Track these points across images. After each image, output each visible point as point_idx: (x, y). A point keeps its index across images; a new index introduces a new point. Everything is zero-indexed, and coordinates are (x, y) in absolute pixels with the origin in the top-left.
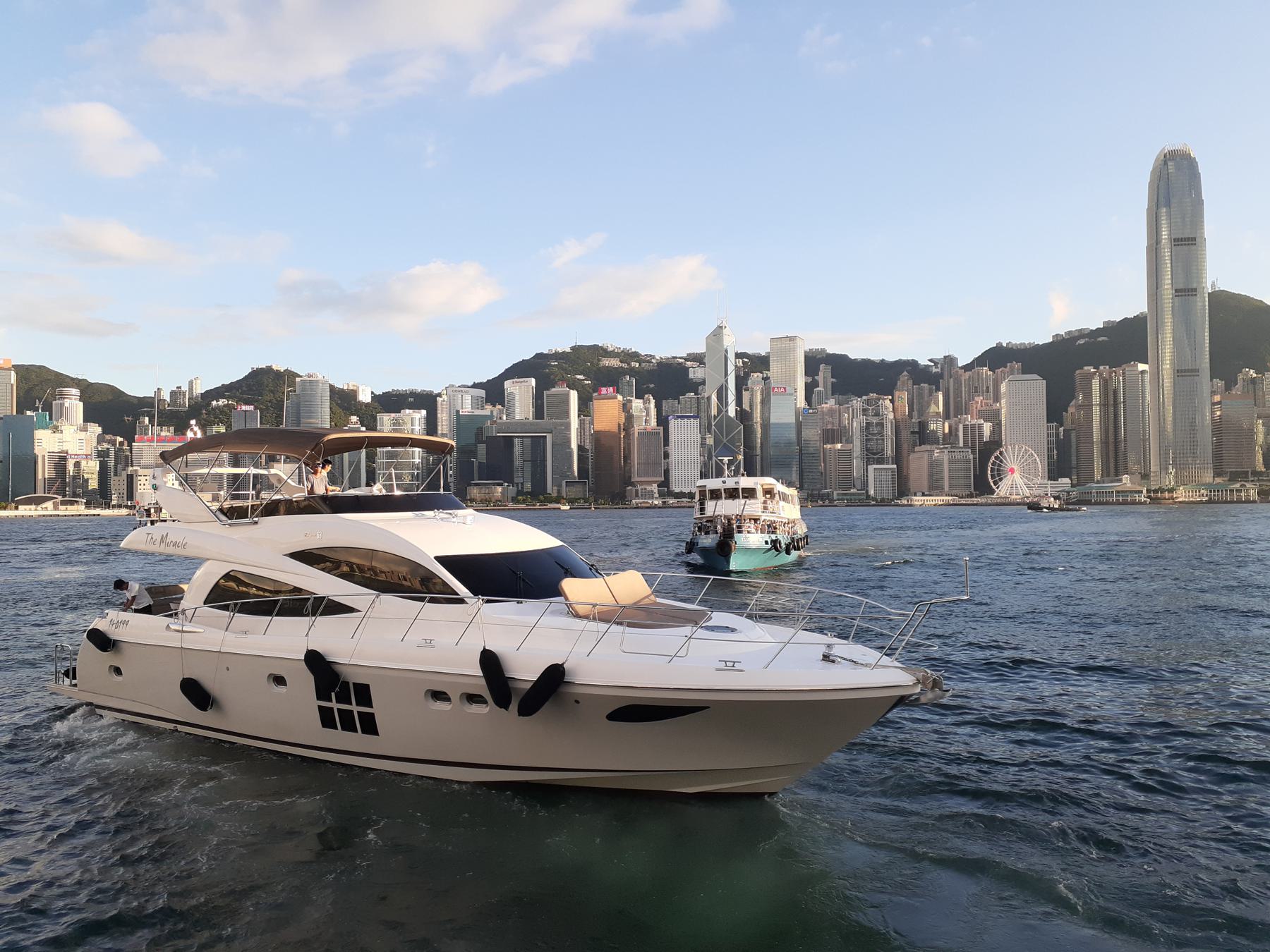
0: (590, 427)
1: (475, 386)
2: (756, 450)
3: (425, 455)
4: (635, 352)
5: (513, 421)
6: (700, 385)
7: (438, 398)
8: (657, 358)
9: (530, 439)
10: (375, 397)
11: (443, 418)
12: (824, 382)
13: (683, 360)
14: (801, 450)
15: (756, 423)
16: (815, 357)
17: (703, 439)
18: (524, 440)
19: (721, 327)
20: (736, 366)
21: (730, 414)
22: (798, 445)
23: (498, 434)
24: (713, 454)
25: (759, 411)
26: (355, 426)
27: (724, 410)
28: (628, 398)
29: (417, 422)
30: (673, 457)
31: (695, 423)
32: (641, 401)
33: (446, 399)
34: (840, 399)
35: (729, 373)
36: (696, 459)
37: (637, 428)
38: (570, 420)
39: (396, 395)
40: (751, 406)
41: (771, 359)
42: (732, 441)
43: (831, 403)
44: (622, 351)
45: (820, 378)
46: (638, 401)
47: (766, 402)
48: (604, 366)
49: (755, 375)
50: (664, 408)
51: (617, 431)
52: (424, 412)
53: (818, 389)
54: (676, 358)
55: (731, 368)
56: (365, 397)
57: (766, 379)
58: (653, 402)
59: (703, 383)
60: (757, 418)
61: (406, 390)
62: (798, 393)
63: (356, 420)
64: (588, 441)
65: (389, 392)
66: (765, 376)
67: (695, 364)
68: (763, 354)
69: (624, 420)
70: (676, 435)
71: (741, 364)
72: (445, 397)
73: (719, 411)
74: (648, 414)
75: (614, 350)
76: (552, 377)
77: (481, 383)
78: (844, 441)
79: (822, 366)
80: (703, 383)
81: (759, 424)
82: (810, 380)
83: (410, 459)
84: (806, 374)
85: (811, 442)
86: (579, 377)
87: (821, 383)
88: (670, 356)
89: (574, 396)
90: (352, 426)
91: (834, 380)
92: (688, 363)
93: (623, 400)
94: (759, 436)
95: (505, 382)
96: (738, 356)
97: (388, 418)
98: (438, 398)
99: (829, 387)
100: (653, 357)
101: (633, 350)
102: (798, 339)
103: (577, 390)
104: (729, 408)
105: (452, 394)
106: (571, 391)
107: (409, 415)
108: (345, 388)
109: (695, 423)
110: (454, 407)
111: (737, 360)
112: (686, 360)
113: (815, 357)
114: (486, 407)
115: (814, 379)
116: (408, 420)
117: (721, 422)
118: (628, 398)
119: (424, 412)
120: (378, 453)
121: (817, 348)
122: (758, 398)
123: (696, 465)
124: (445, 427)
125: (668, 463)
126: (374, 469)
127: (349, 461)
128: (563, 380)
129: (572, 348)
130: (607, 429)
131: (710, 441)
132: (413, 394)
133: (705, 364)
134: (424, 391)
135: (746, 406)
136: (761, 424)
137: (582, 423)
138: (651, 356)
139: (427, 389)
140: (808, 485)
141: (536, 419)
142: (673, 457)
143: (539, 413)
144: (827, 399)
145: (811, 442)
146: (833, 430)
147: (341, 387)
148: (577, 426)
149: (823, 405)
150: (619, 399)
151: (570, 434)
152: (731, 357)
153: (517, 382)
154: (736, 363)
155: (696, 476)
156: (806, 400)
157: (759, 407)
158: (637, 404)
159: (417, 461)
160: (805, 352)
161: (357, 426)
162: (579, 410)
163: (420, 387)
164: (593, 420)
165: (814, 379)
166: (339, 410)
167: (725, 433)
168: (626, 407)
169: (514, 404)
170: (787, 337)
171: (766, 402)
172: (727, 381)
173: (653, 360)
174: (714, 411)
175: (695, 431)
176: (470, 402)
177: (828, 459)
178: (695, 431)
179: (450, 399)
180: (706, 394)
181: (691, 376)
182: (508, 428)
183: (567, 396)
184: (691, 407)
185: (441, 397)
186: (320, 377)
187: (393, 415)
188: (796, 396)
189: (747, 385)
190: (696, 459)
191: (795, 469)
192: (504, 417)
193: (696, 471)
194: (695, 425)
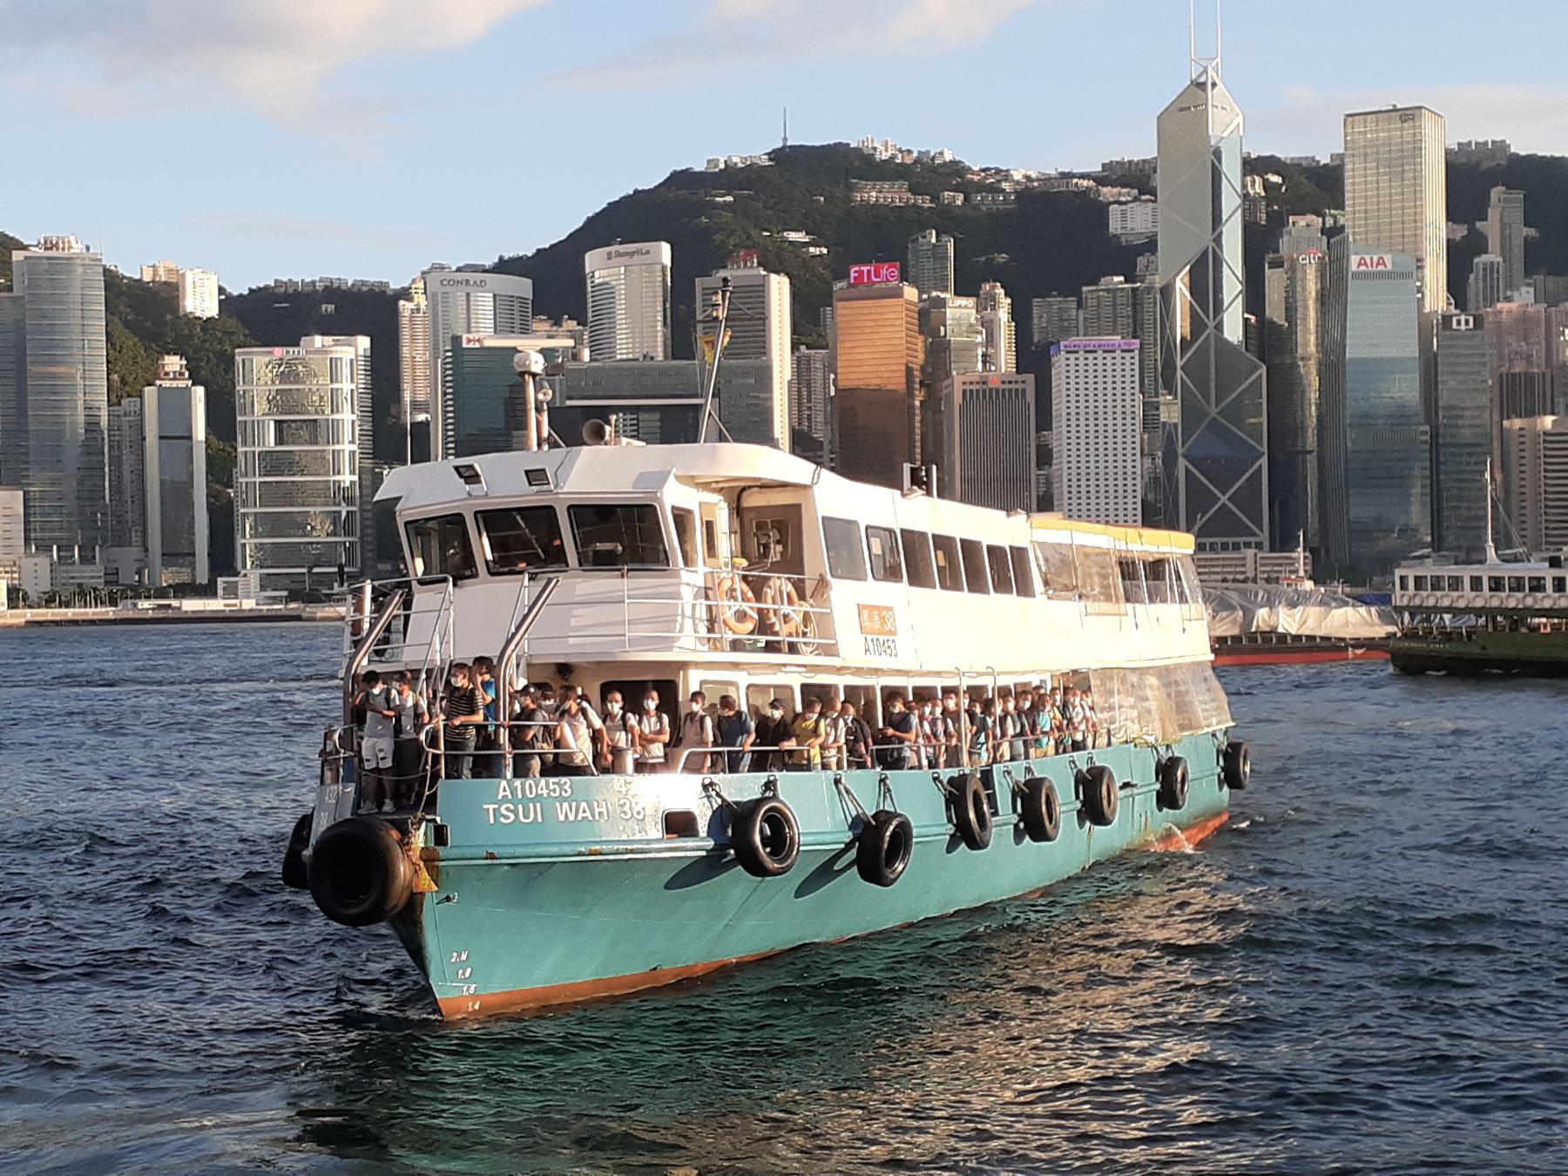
0: (826, 379)
1: (505, 266)
2: (1304, 436)
3: (368, 463)
4: (953, 163)
5: (608, 363)
6: (1142, 255)
7: (402, 302)
8: (1017, 176)
9: (657, 416)
10: (228, 302)
11: (416, 353)
12: (1503, 238)
13: (1092, 182)
14: (1435, 435)
15: (1302, 359)
16: (1478, 164)
17: (1150, 408)
18: (643, 416)
19: (1201, 86)
20: (1246, 196)
21: (1226, 335)
22: (1427, 423)
23: (569, 403)
24: (1180, 451)
25: (1312, 325)
26: (175, 384)
27: (1211, 324)
28: (934, 294)
29: (346, 371)
30: (1065, 459)
31: (1128, 361)
32: (970, 302)
33: (423, 307)
34: (1550, 286)
35: (1224, 217)
36: (1129, 464)
37: (959, 380)
38: (770, 360)
39: (286, 297)
40: (1290, 310)
41: (1348, 167)
42: (1235, 412)
43: (1521, 300)
44: (916, 162)
45: (1490, 227)
46: (963, 301)
47: (1333, 296)
48: (865, 205)
49: (1302, 221)
50: (1036, 321)
51: (904, 387)
52: (364, 342)
53: (1484, 258)
54: (1070, 176)
55: (1230, 202)
56: (201, 302)
57: (1332, 232)
58: (1005, 302)
59: (1151, 246)
60: (1306, 345)
61: (313, 283)
62: (1427, 271)
63: (177, 368)
64: (820, 419)
65: (267, 288)
66: (1330, 222)
67: (1126, 193)
68: (1324, 160)
69: (921, 356)
70: (1073, 398)
71: (1259, 189)
72: (421, 300)
73: (1197, 325)
74: (990, 340)
75: (893, 157)
76: (718, 237)
77: (521, 258)
78: (1561, 408)
79: (1496, 193)
80: (1151, 246)
81: (1312, 362)
82: (1461, 231)
83: (327, 474)
84: (1450, 216)
85: (1466, 413)
86: (794, 236)
87: (1494, 242)
88: (1053, 173)
89: (779, 290)
90: (166, 384)
91: (1532, 232)
92: (1105, 190)
93: (921, 300)
94: (1313, 396)
95: (588, 256)
96: (1252, 166)
97: (267, 359)
98: (402, 302)
99: (1518, 251)
100: (1007, 176)
101: (948, 157)
102: (1427, 121)
103: (788, 275)
104: (1226, 317)
105: (440, 290)
106: (773, 277)
107: (323, 351)
108: (147, 278)
109: (1128, 361)
110: (447, 327)
111: (1249, 178)
112: (1100, 180)
113: (1478, 164)
114: (535, 326)
115: (1472, 230)
116: (320, 365)
117: (1203, 351)
118: (934, 294)
119: (364, 342)
120: (241, 458)
121: (1481, 140)
122: (1311, 285)
123: (1129, 482)
124: (421, 383)
125: (1048, 482)
126: (230, 502)
127: (162, 483)
128: (750, 246)
129: (775, 155)
130: (874, 382)
131: (1170, 412)
132: (333, 292)
133: (1153, 192)
134: (364, 283)
135: (1275, 311)
136: (1320, 364)
137: (802, 369)
138: (998, 171)
139: (372, 279)
140: (1457, 538)
141: (675, 357)
142: (1065, 459)
143: (681, 341)
144: (1510, 286)
145: (1466, 413)
146: (1529, 378)
147: (137, 277)
148: (788, 376)
149: (1499, 306)
150: (906, 296)
151: (770, 399)
152: (1231, 169)
153: (619, 255)
154: (1244, 186)
155: (1130, 512)
156: (1449, 290)
157: (1312, 314)
158: (959, 311)
159: (347, 478)
160: (1448, 152)
161: (182, 384)
162: (794, 332)
163: (352, 271)
164: (833, 358)
165: (1472, 230)
166: (130, 341)
167: (1213, 391)
168: (928, 319)
169: (612, 318)
170: (1395, 110)
171: (1333, 296)
172: (1218, 240)
173: (1005, 185)
174: (1181, 327)
175: (1128, 386)
176: (490, 314)
177: (1514, 461)
178: (1128, 386)
179: (435, 306)
180: (1157, 278)
181: (1114, 226)
182: (597, 384)
183: (759, 294)
184: (1115, 317)
185: (409, 298)
186: (77, 248)
187: (279, 352)
188: (1422, 280)
189: (1276, 251)
190: (1129, 464)
191: (1418, 489)
192: (586, 355)
193: (1130, 500)
194: (1128, 367)
